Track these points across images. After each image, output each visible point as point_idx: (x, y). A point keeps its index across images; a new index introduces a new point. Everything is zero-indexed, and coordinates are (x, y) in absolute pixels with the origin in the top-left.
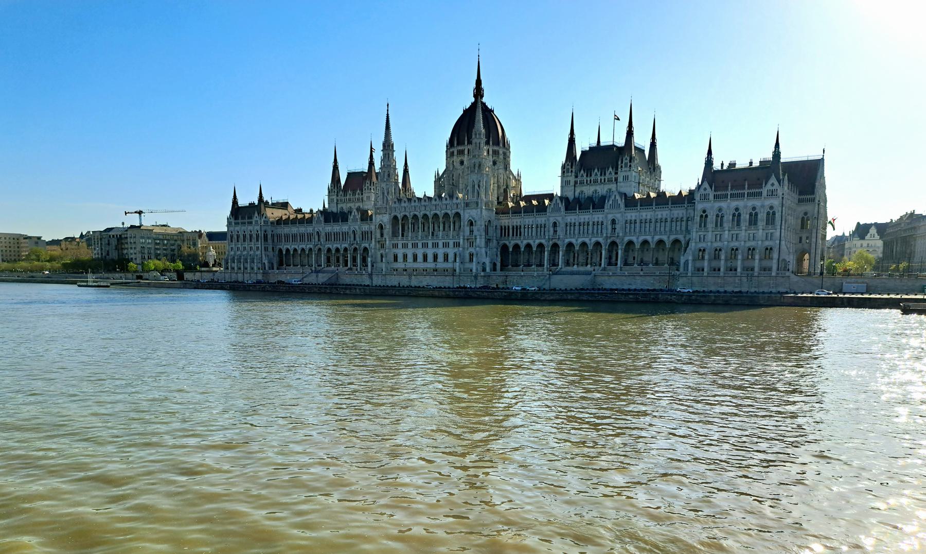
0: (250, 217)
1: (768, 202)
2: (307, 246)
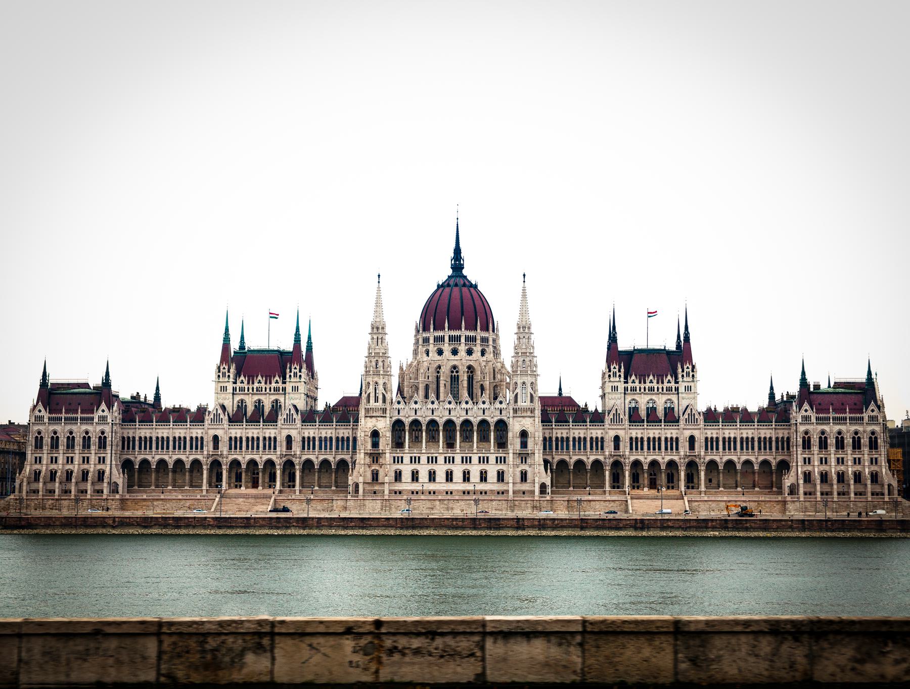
1: (870, 428)
2: (187, 457)
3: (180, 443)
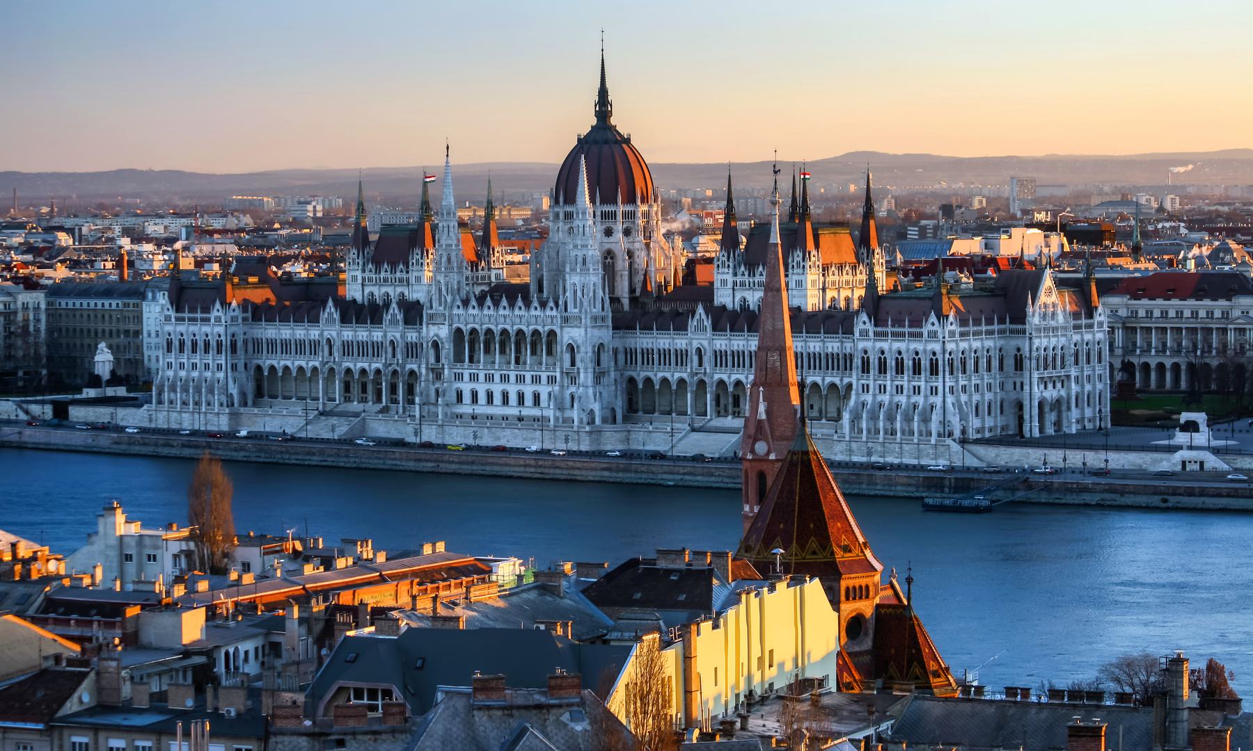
0: (206, 310)
2: (308, 363)
3: (300, 347)
